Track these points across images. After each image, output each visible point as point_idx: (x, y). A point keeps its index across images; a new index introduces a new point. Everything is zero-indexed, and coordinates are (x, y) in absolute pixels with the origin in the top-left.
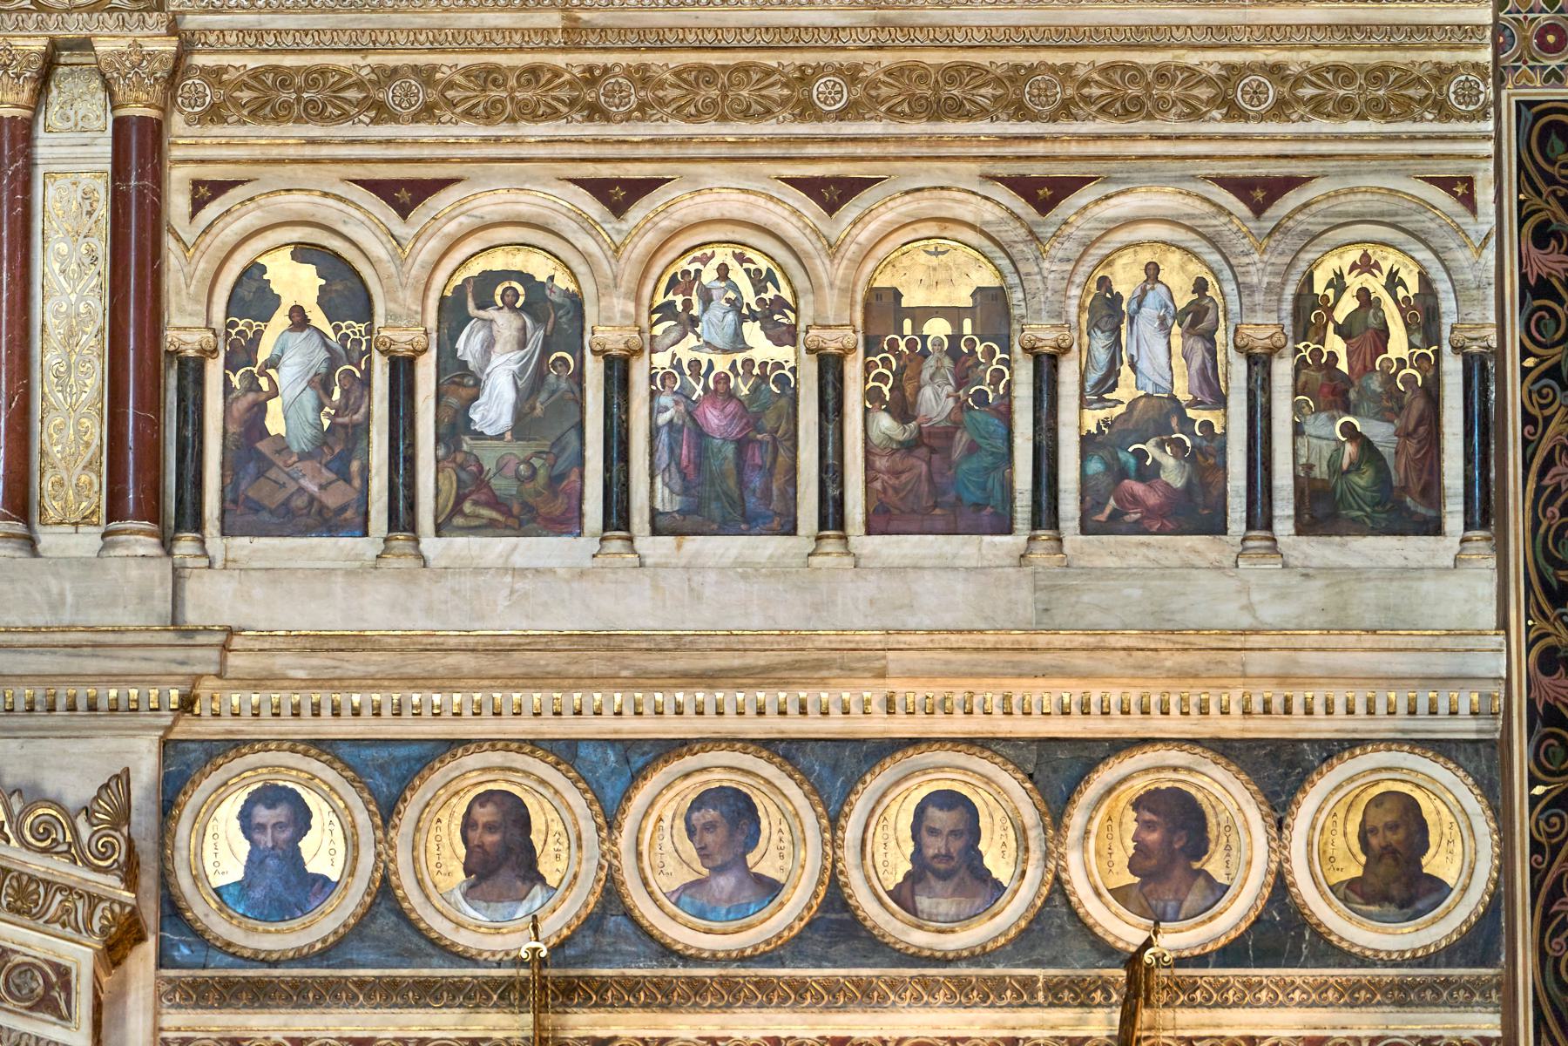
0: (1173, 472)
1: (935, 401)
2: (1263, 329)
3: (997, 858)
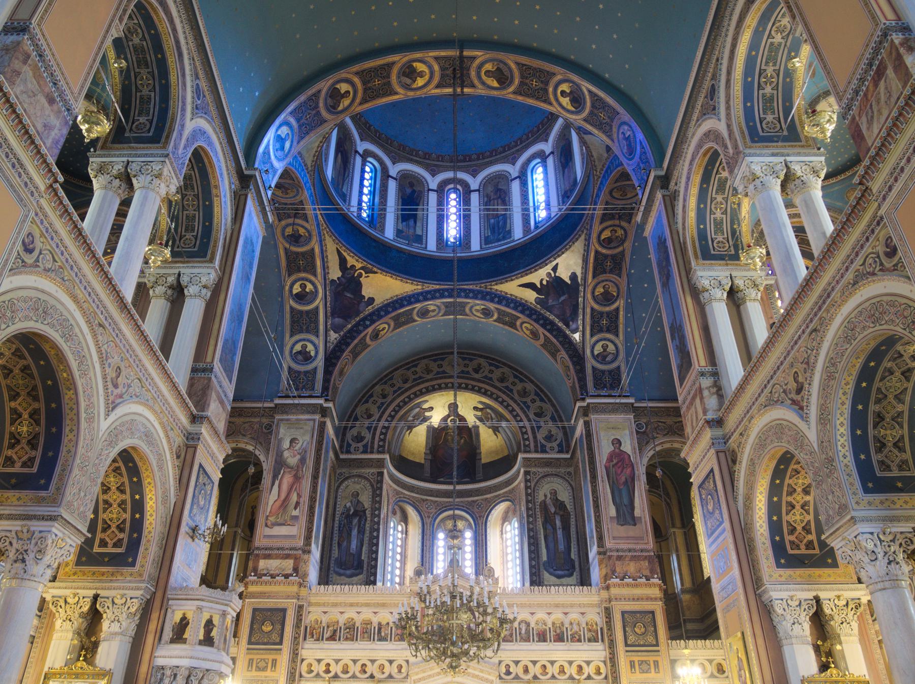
0: (577, 637)
1: (558, 631)
2: (584, 625)
3: (566, 671)
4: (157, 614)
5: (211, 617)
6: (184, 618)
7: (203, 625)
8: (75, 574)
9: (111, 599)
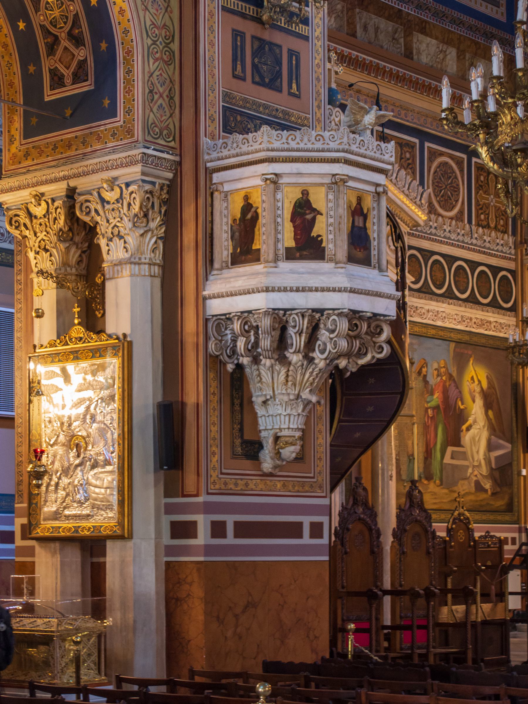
4: (193, 206)
5: (305, 193)
6: (247, 207)
7: (287, 215)
8: (27, 155)
9: (95, 194)
